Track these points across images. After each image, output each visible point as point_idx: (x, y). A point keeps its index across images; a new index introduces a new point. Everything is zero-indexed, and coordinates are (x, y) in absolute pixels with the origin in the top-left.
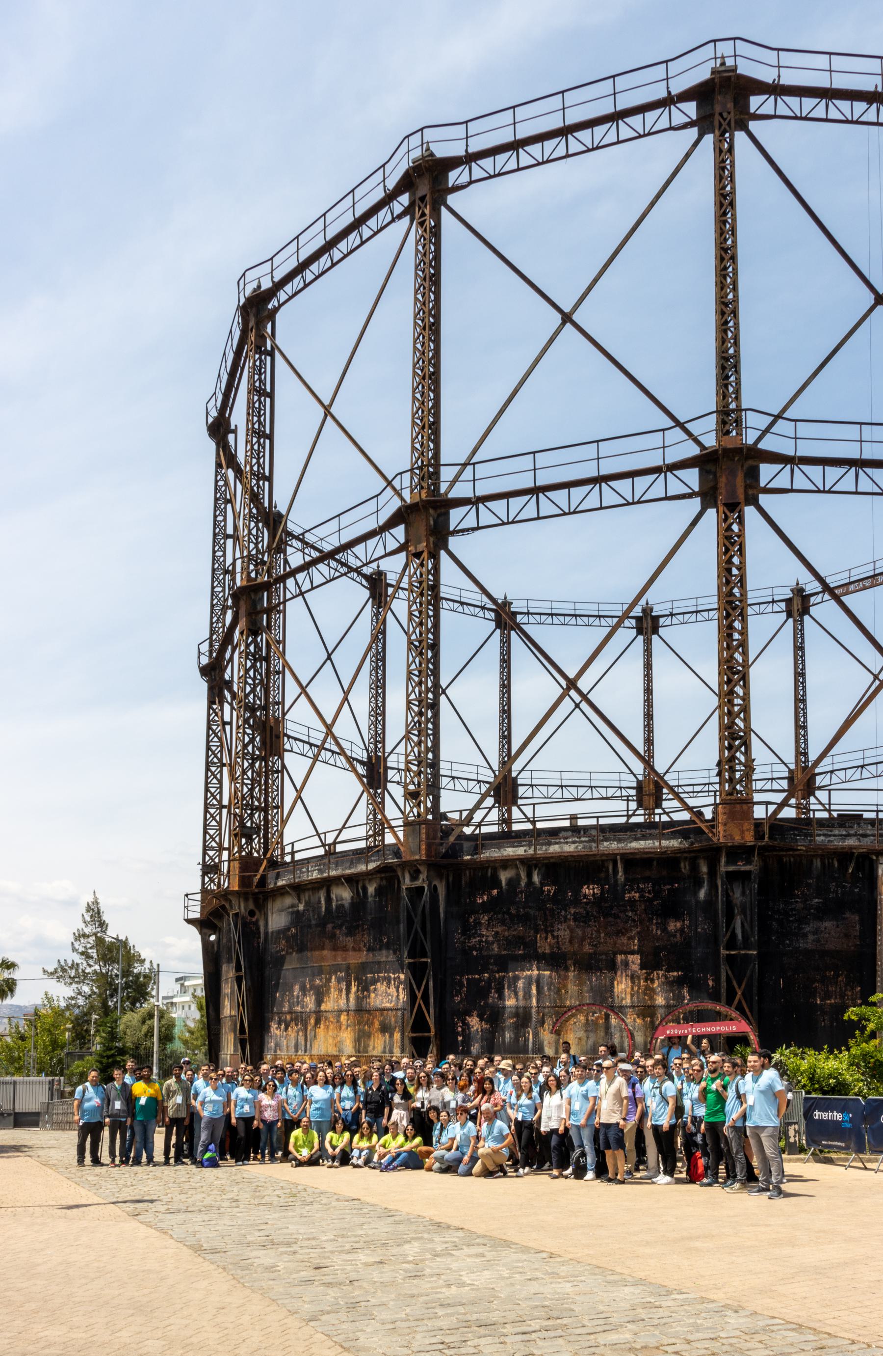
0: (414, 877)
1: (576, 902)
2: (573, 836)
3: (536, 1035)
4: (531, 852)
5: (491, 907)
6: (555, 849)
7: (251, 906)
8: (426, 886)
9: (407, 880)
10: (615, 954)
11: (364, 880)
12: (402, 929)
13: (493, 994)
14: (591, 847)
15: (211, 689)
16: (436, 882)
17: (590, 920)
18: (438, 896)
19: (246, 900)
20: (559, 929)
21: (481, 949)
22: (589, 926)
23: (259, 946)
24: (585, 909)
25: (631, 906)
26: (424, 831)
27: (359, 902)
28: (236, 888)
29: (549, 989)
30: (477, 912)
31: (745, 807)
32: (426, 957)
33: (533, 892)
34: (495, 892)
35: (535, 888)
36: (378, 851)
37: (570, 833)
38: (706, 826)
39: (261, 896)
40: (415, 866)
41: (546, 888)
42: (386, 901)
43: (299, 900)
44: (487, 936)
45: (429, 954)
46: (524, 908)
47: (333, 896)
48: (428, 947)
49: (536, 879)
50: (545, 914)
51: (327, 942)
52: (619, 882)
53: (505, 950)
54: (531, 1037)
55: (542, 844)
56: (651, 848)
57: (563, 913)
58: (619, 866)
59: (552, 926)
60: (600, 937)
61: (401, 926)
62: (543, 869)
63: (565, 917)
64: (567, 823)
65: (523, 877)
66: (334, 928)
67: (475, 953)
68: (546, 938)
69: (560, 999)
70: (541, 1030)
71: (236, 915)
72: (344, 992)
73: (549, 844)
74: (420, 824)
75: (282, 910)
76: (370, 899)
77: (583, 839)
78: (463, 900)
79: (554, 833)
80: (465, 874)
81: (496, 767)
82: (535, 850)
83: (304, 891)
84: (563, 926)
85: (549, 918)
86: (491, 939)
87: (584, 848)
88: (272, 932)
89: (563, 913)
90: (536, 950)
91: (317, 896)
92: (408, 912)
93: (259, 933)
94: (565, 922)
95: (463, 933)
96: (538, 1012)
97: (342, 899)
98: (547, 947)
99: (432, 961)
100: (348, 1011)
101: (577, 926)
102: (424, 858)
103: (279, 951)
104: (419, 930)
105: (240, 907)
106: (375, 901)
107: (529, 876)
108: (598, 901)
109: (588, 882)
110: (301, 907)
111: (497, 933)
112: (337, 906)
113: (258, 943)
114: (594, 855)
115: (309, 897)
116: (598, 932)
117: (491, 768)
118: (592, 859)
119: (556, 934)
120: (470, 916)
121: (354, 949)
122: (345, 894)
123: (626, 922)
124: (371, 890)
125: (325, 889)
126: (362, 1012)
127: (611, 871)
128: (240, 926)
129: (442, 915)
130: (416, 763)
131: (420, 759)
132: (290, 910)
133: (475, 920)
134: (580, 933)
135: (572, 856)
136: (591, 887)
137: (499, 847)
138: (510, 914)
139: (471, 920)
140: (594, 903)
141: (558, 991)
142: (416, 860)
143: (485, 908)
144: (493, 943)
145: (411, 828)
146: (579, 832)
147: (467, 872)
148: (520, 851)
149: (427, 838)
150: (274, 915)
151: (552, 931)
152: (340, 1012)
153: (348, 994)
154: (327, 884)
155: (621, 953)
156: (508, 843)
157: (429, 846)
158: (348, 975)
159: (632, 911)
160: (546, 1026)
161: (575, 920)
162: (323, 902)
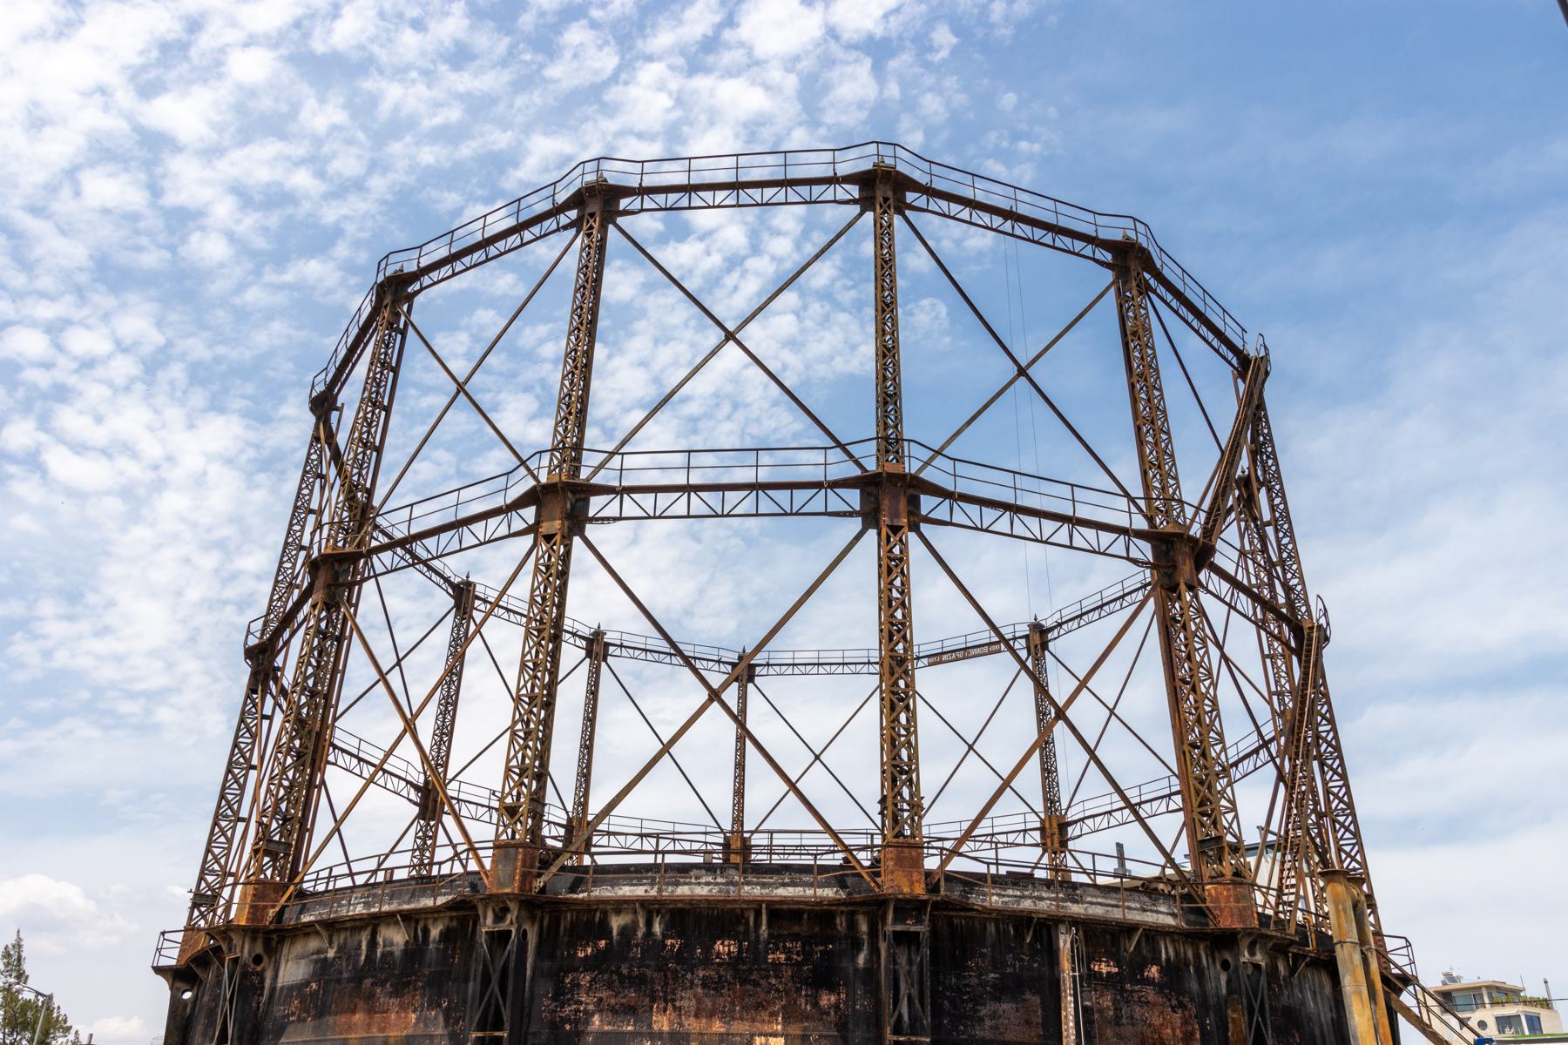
0: (499, 918)
1: (706, 962)
2: (707, 875)
4: (653, 893)
5: (596, 963)
6: (683, 891)
7: (259, 949)
8: (514, 930)
9: (489, 921)
10: (753, 1035)
11: (425, 919)
12: (470, 989)
14: (728, 892)
15: (254, 675)
16: (526, 926)
17: (723, 987)
18: (527, 944)
19: (254, 940)
20: (682, 998)
21: (577, 1021)
22: (721, 995)
23: (258, 1008)
24: (718, 973)
25: (775, 971)
26: (520, 857)
27: (415, 951)
28: (243, 923)
30: (576, 970)
31: (914, 853)
32: (501, 1030)
33: (653, 946)
34: (603, 942)
35: (655, 941)
36: (451, 881)
37: (704, 872)
38: (867, 873)
39: (275, 936)
40: (504, 902)
41: (669, 942)
42: (454, 950)
43: (331, 943)
44: (587, 1004)
45: (507, 1026)
46: (638, 967)
47: (380, 940)
48: (506, 1016)
49: (657, 928)
50: (666, 976)
51: (361, 1004)
52: (762, 939)
53: (609, 1024)
55: (668, 884)
56: (802, 896)
57: (689, 976)
58: (764, 917)
59: (674, 994)
60: (734, 1011)
61: (471, 984)
62: (668, 917)
63: (692, 982)
64: (699, 859)
65: (641, 925)
66: (374, 984)
67: (568, 1027)
68: (665, 1010)
71: (235, 961)
73: (677, 884)
74: (516, 846)
75: (303, 958)
76: (431, 946)
77: (719, 880)
78: (558, 953)
79: (684, 869)
80: (566, 917)
81: (570, 808)
82: (660, 890)
83: (339, 931)
84: (688, 994)
85: (671, 982)
86: (591, 1007)
87: (720, 891)
88: (282, 988)
89: (689, 976)
90: (650, 1026)
91: (357, 938)
92: (485, 965)
93: (262, 988)
94: (691, 988)
95: (555, 998)
97: (392, 944)
98: (665, 1023)
99: (509, 1035)
101: (706, 995)
102: (516, 892)
103: (288, 1016)
104: (497, 991)
105: (244, 950)
106: (437, 949)
107: (649, 924)
108: (735, 962)
109: (722, 937)
110: (331, 954)
111: (601, 1000)
112: (383, 954)
113: (259, 1003)
114: (735, 900)
115: (346, 940)
116: (733, 1003)
117: (565, 809)
118: (729, 906)
119: (678, 1004)
120: (566, 975)
122: (396, 937)
123: (769, 992)
124: (435, 932)
125: (369, 930)
127: (751, 923)
128: (237, 977)
129: (529, 972)
130: (517, 771)
131: (523, 766)
132: (315, 957)
133: (572, 980)
134: (709, 1004)
135: (707, 901)
136: (726, 943)
137: (614, 884)
138: (620, 974)
139: (568, 981)
140: (729, 964)
142: (507, 894)
143: (588, 965)
144: (593, 1014)
145: (502, 851)
146: (715, 872)
147: (569, 915)
148: (640, 891)
149: (524, 866)
150: (290, 963)
151: (674, 1000)
154: (374, 922)
155: (761, 1035)
156: (624, 879)
157: (524, 876)
159: (776, 977)
161: (704, 986)
162: (364, 947)
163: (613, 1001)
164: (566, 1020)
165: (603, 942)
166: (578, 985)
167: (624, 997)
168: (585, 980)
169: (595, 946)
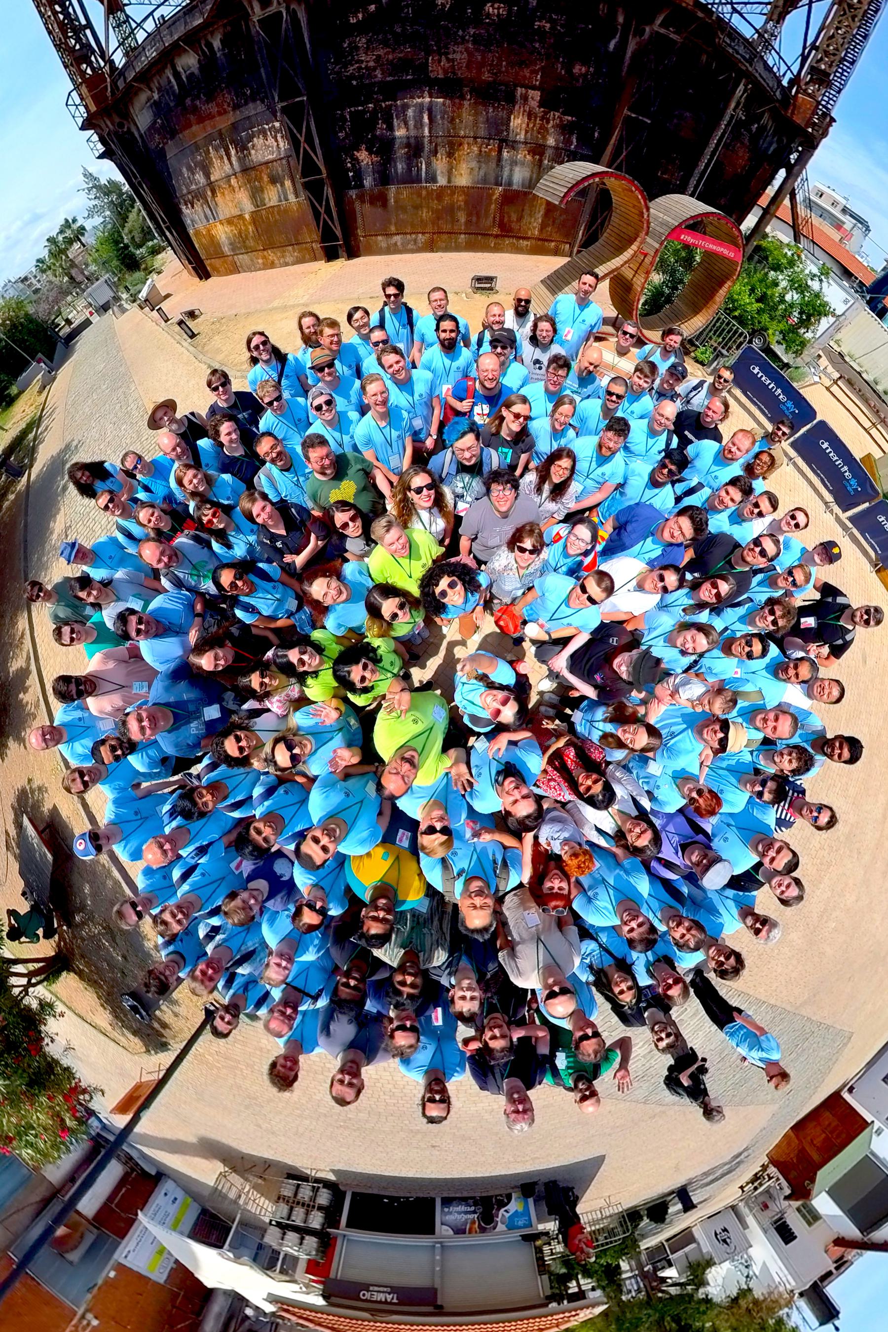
3: (429, 164)
13: (381, 125)
27: (208, 62)
29: (443, 118)
54: (424, 167)
69: (454, 129)
70: (433, 159)
72: (225, 158)
96: (431, 142)
100: (235, 174)
121: (220, 114)
124: (217, 43)
126: (248, 170)
141: (452, 120)
152: (228, 177)
153: (229, 159)
158: (222, 139)
160: (439, 155)
163: (390, 57)
164: (352, 77)
165: (372, 7)
166: (357, 48)
167: (401, 52)
168: (362, 42)
169: (365, 11)
